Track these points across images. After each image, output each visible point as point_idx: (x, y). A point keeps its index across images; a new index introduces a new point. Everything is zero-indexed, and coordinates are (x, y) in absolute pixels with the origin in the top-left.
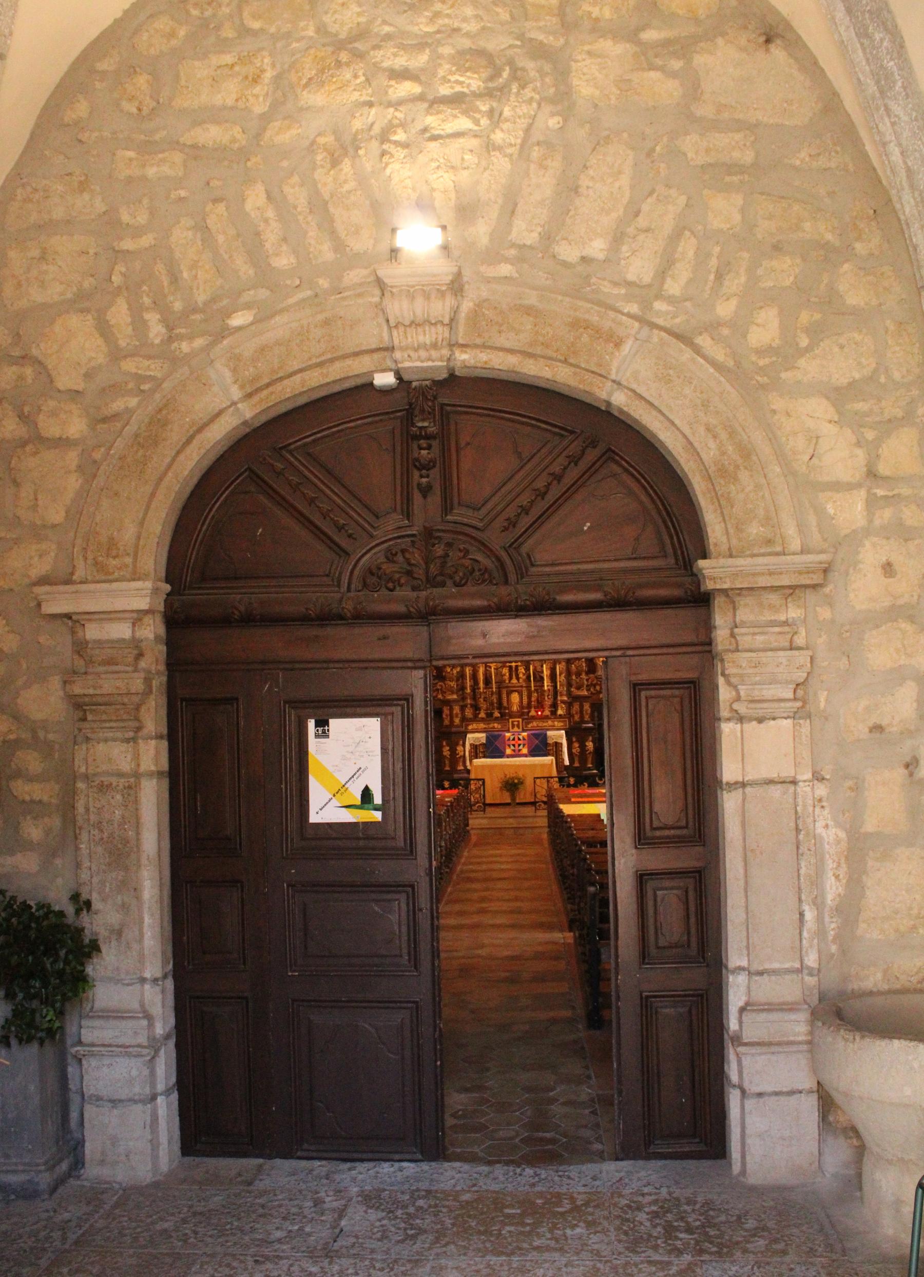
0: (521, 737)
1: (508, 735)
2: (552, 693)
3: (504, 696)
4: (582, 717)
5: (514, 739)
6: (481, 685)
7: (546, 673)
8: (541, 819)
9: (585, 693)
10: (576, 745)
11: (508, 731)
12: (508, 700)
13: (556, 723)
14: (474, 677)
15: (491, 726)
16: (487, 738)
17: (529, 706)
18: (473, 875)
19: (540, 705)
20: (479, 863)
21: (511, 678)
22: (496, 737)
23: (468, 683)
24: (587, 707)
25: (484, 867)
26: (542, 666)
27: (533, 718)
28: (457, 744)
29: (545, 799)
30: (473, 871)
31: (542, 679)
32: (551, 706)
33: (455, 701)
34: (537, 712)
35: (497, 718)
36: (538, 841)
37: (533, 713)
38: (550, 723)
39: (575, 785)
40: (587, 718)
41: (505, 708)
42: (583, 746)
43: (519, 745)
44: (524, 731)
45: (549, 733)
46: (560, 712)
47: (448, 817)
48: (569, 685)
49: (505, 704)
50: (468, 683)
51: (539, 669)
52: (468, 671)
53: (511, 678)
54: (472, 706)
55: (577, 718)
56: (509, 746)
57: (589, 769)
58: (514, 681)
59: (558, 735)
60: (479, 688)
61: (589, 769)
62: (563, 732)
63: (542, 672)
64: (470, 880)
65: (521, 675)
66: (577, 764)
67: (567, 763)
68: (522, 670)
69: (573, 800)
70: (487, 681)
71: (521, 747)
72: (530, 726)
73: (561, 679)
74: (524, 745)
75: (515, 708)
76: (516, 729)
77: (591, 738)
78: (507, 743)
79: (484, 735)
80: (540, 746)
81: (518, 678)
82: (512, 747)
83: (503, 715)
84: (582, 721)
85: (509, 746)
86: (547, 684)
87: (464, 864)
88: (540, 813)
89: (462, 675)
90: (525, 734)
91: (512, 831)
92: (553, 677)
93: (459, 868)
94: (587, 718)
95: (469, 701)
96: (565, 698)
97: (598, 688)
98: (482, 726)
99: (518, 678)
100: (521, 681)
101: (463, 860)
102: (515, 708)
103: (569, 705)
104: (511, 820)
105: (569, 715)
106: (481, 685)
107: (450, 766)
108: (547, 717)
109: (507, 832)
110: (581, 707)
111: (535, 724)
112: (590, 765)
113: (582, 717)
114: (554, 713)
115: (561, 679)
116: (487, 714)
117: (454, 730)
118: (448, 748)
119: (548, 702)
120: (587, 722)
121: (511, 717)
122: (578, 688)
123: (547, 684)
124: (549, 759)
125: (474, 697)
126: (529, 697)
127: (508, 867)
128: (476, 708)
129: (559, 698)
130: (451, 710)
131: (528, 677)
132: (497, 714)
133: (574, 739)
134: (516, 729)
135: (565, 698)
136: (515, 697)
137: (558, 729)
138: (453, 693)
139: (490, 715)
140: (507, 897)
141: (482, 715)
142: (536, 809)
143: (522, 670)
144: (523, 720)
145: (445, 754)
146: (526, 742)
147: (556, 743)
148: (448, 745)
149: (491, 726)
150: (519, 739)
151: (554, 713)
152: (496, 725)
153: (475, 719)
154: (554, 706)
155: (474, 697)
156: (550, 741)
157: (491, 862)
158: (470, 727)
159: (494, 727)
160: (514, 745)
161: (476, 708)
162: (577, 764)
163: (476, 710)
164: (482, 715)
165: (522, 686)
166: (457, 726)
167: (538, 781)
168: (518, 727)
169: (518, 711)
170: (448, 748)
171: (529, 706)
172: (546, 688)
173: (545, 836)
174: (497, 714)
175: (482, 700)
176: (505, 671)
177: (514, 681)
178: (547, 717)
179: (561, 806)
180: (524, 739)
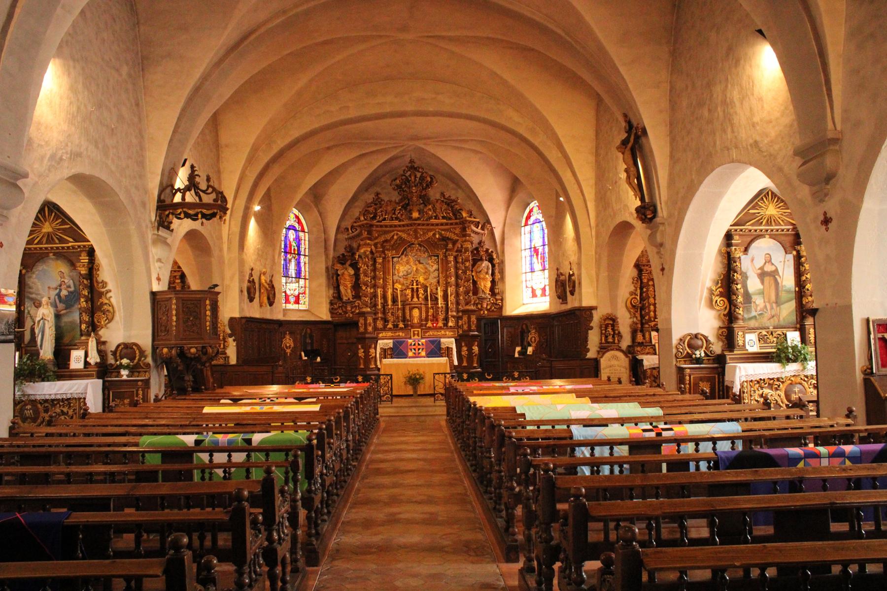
0: (420, 343)
1: (410, 341)
2: (444, 309)
3: (407, 312)
4: (469, 326)
5: (415, 345)
6: (390, 302)
7: (440, 294)
8: (440, 408)
9: (472, 307)
10: (465, 349)
11: (410, 338)
12: (411, 315)
13: (447, 333)
14: (384, 297)
15: (397, 334)
16: (394, 343)
17: (427, 320)
18: (382, 466)
19: (435, 319)
20: (387, 451)
21: (412, 297)
22: (401, 343)
23: (380, 301)
24: (473, 318)
25: (392, 456)
26: (437, 289)
27: (429, 328)
28: (370, 347)
29: (443, 391)
30: (382, 461)
31: (437, 299)
32: (443, 320)
33: (368, 313)
34: (433, 324)
35: (401, 329)
36: (439, 429)
37: (429, 324)
38: (443, 332)
39: (468, 380)
40: (473, 327)
42: (470, 350)
43: (419, 349)
44: (422, 338)
45: (442, 340)
46: (450, 324)
47: (357, 409)
48: (458, 303)
49: (408, 317)
50: (380, 301)
51: (434, 291)
52: (379, 291)
53: (412, 297)
54: (382, 318)
55: (465, 327)
56: (411, 350)
57: (475, 368)
58: (415, 299)
59: (449, 342)
60: (388, 305)
61: (475, 368)
62: (453, 340)
63: (437, 294)
64: (379, 472)
65: (420, 295)
66: (465, 364)
67: (456, 363)
68: (421, 291)
69: (475, 392)
70: (394, 300)
71: (420, 351)
73: (451, 298)
74: (423, 349)
75: (416, 321)
76: (416, 337)
77: (476, 343)
78: (410, 347)
79: (391, 341)
80: (435, 350)
81: (418, 298)
82: (413, 351)
83: (406, 326)
84: (470, 329)
85: (411, 350)
86: (440, 302)
87: (374, 452)
88: (438, 403)
89: (375, 295)
90: (423, 341)
91: (414, 419)
92: (445, 297)
93: (368, 457)
94: (473, 327)
95: (380, 315)
96: (455, 314)
97: (479, 306)
98: (390, 334)
99: (418, 298)
100: (420, 300)
101: (372, 448)
102: (416, 321)
103: (458, 318)
104: (414, 409)
105: (457, 326)
106: (390, 302)
107: (364, 365)
108: (441, 328)
109: (411, 419)
110: (469, 318)
111: (431, 333)
112: (475, 365)
113: (469, 326)
114: (446, 325)
115: (451, 298)
116: (394, 325)
117: (367, 336)
118: (362, 350)
119: (441, 316)
120: (473, 331)
121: (412, 327)
122: (467, 304)
123: (440, 302)
124: (444, 360)
125: (384, 313)
126: (427, 312)
127: (414, 456)
128: (386, 321)
129: (450, 313)
130: (366, 320)
131: (426, 299)
132: (401, 325)
134: (416, 337)
135: (455, 314)
136: (416, 312)
137: (449, 337)
138: (367, 306)
139: (396, 326)
140: (419, 498)
141: (390, 326)
142: (435, 400)
143: (421, 291)
144: (422, 329)
145: (360, 355)
146: (424, 347)
147: (448, 347)
148: (362, 348)
149: (397, 334)
150: (419, 345)
151: (446, 325)
152: (401, 334)
153: (385, 328)
154: (446, 319)
155: (384, 313)
156: (443, 346)
157: (399, 451)
158: (381, 335)
160: (415, 349)
161: (386, 321)
162: (465, 364)
163: (385, 322)
164: (390, 326)
165: (421, 304)
166: (370, 333)
167: (437, 376)
168: (418, 335)
170: (362, 350)
171: (427, 320)
172: (440, 305)
173: (443, 423)
174: (401, 325)
175: (390, 314)
176: (409, 292)
177: (415, 299)
178: (441, 328)
179: (472, 399)
180: (423, 344)
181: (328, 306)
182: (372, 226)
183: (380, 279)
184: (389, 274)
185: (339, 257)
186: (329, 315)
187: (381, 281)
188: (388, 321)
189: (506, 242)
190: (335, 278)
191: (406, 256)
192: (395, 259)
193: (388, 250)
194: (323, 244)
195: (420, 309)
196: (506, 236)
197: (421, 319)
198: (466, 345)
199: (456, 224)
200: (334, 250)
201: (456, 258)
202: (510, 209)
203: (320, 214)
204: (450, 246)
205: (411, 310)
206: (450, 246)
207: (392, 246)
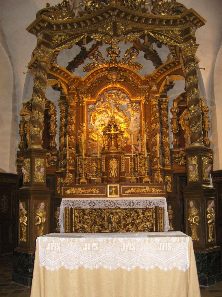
13: (153, 189)
15: (89, 191)
33: (37, 151)
41: (104, 174)
49: (104, 170)
72: (129, 191)
75: (113, 174)
100: (119, 149)
102: (113, 174)
107: (27, 238)
121: (110, 182)
130: (32, 163)
133: (191, 203)
149: (89, 191)
152: (94, 191)
158: (68, 192)
159: (92, 192)
166: (39, 184)
169: (116, 177)
181: (15, 158)
182: (50, 26)
183: (71, 125)
184: (83, 121)
185: (28, 103)
186: (16, 168)
187: (73, 127)
188: (80, 175)
189: (216, 88)
190: (22, 127)
191: (102, 102)
192: (90, 106)
193: (82, 93)
194: (12, 90)
195: (119, 159)
196: (215, 82)
197: (120, 173)
198: (197, 206)
199: (175, 21)
200: (25, 97)
201: (160, 103)
202: (220, 50)
203: (10, 57)
204: (155, 88)
205: (108, 160)
206: (155, 88)
207: (88, 90)
